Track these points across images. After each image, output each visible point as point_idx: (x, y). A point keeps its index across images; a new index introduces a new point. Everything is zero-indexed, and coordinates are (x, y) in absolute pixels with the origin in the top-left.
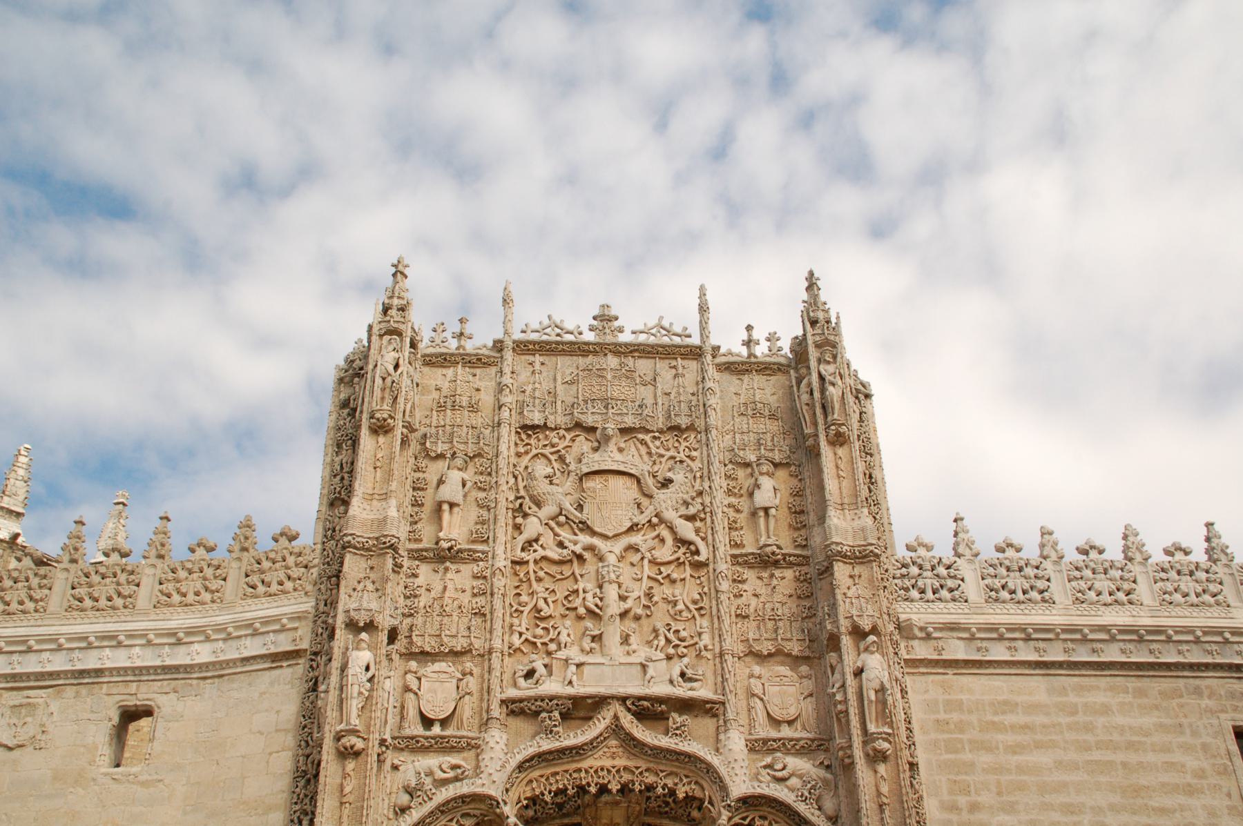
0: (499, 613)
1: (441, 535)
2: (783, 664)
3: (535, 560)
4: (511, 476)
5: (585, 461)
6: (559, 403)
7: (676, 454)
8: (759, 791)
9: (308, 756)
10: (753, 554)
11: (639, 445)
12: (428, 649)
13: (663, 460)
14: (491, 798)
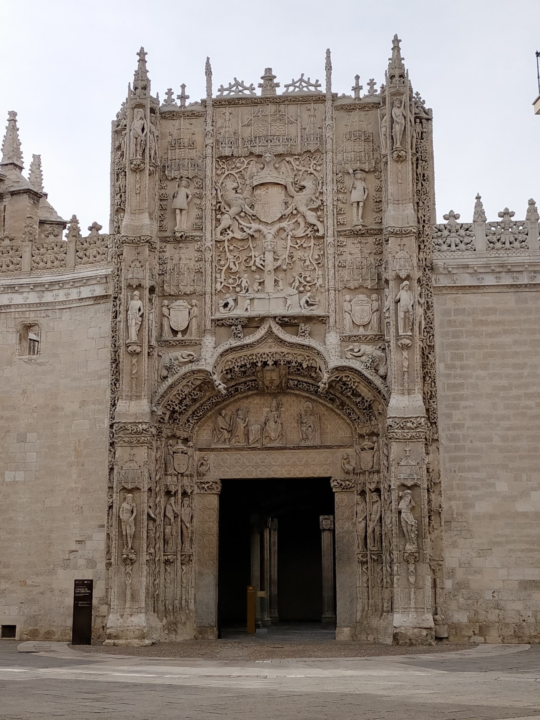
0: (209, 272)
1: (176, 228)
2: (363, 293)
3: (228, 240)
4: (214, 189)
5: (255, 178)
6: (240, 140)
7: (308, 169)
8: (345, 364)
9: (116, 352)
10: (349, 230)
11: (287, 164)
12: (172, 293)
13: (301, 173)
14: (207, 371)
